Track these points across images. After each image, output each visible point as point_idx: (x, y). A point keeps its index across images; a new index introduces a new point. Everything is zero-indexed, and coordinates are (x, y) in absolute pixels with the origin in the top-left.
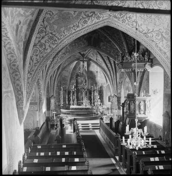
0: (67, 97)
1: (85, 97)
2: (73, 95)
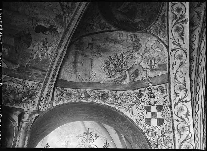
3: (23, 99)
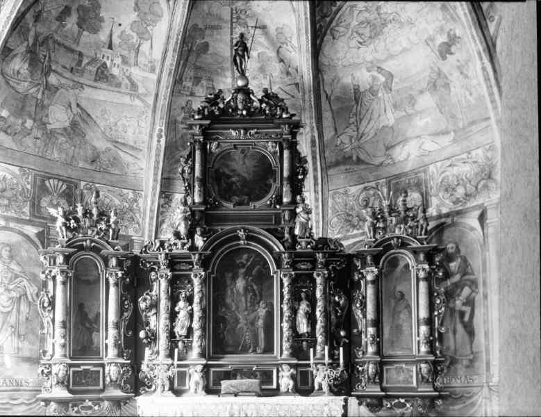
0: (112, 317)
1: (294, 312)
2: (174, 299)
3: (480, 186)
